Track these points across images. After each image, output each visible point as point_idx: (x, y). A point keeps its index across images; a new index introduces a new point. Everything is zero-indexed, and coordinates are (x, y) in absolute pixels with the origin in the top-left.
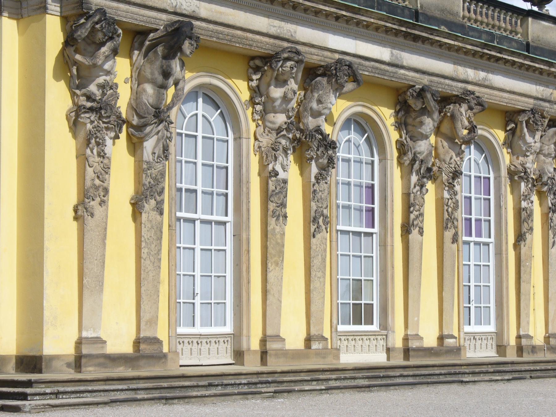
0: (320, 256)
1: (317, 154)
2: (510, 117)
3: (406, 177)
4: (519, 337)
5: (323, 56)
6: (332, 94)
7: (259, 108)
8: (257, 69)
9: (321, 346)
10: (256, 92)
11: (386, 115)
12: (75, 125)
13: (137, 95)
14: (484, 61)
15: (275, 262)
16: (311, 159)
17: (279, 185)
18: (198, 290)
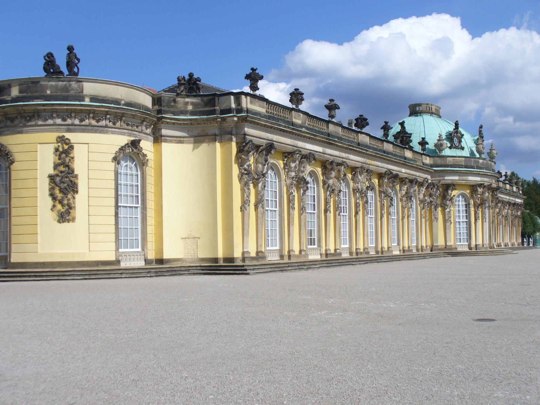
2: (353, 170)
3: (325, 193)
4: (356, 249)
7: (286, 170)
8: (286, 157)
10: (285, 165)
11: (319, 170)
12: (240, 179)
13: (256, 168)
14: (348, 151)
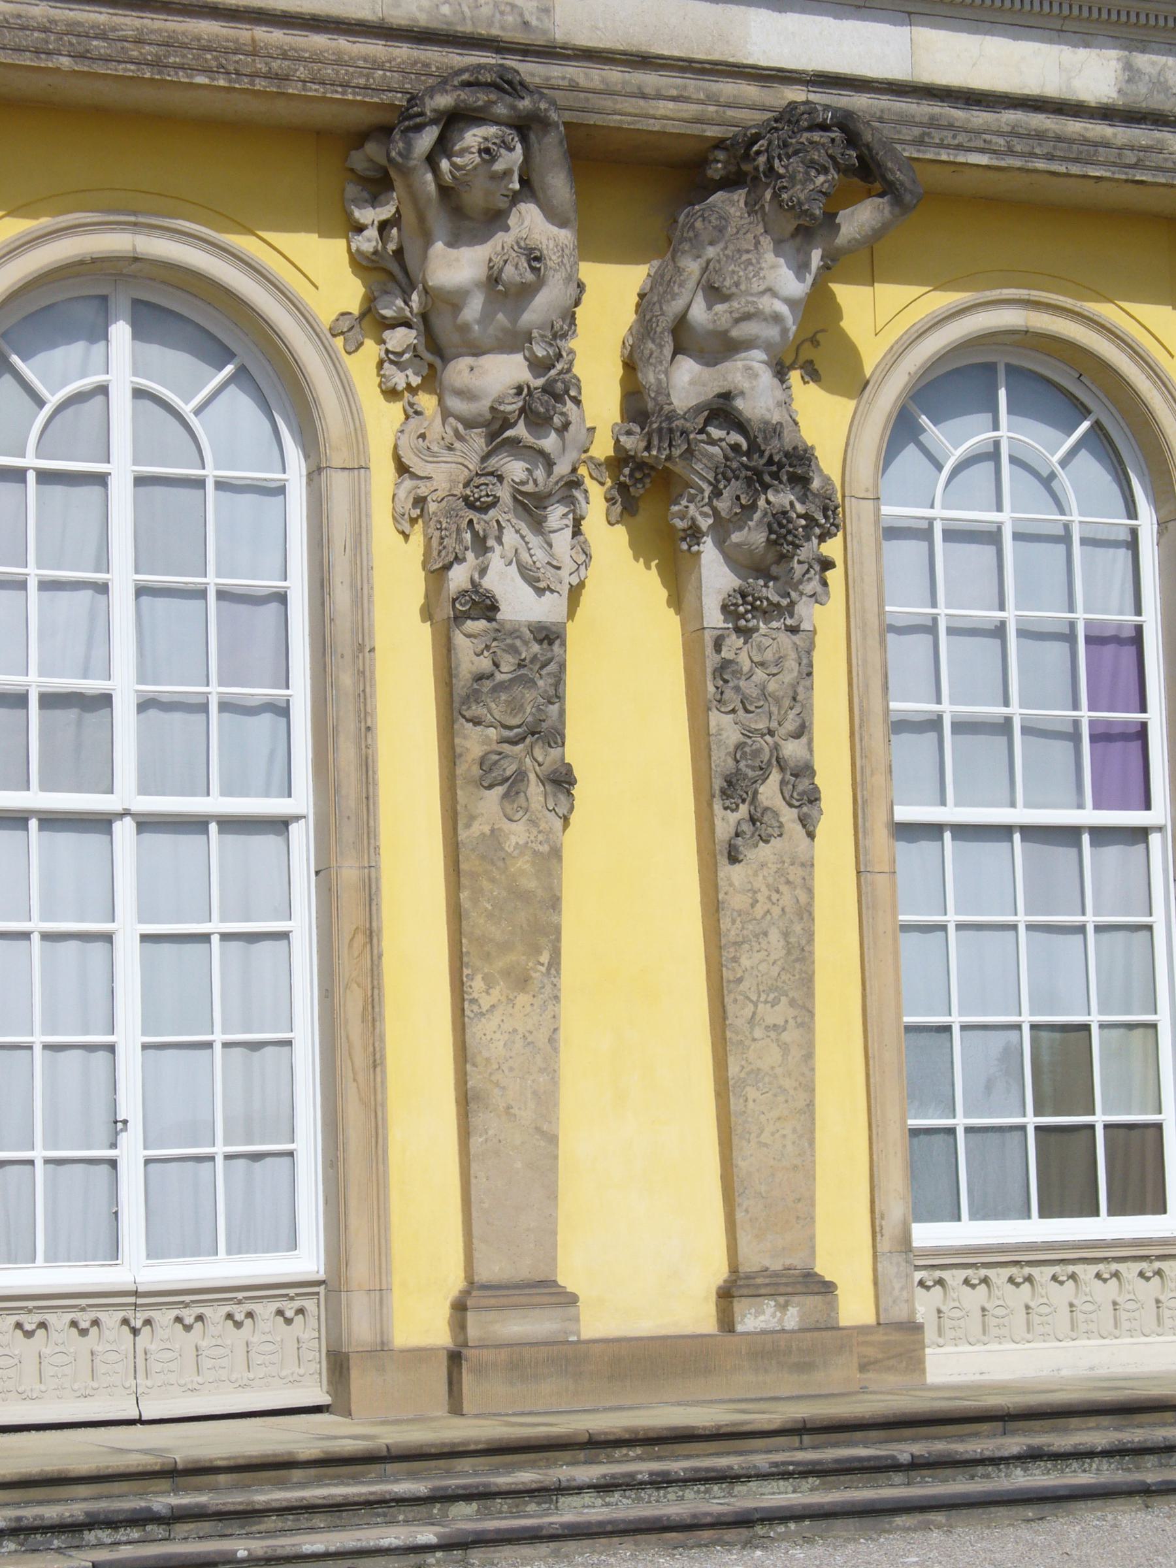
0: (775, 936)
1: (716, 513)
5: (712, 99)
6: (770, 257)
9: (792, 1318)
10: (390, 272)
15: (507, 973)
16: (694, 534)
17: (513, 650)
18: (130, 1106)
